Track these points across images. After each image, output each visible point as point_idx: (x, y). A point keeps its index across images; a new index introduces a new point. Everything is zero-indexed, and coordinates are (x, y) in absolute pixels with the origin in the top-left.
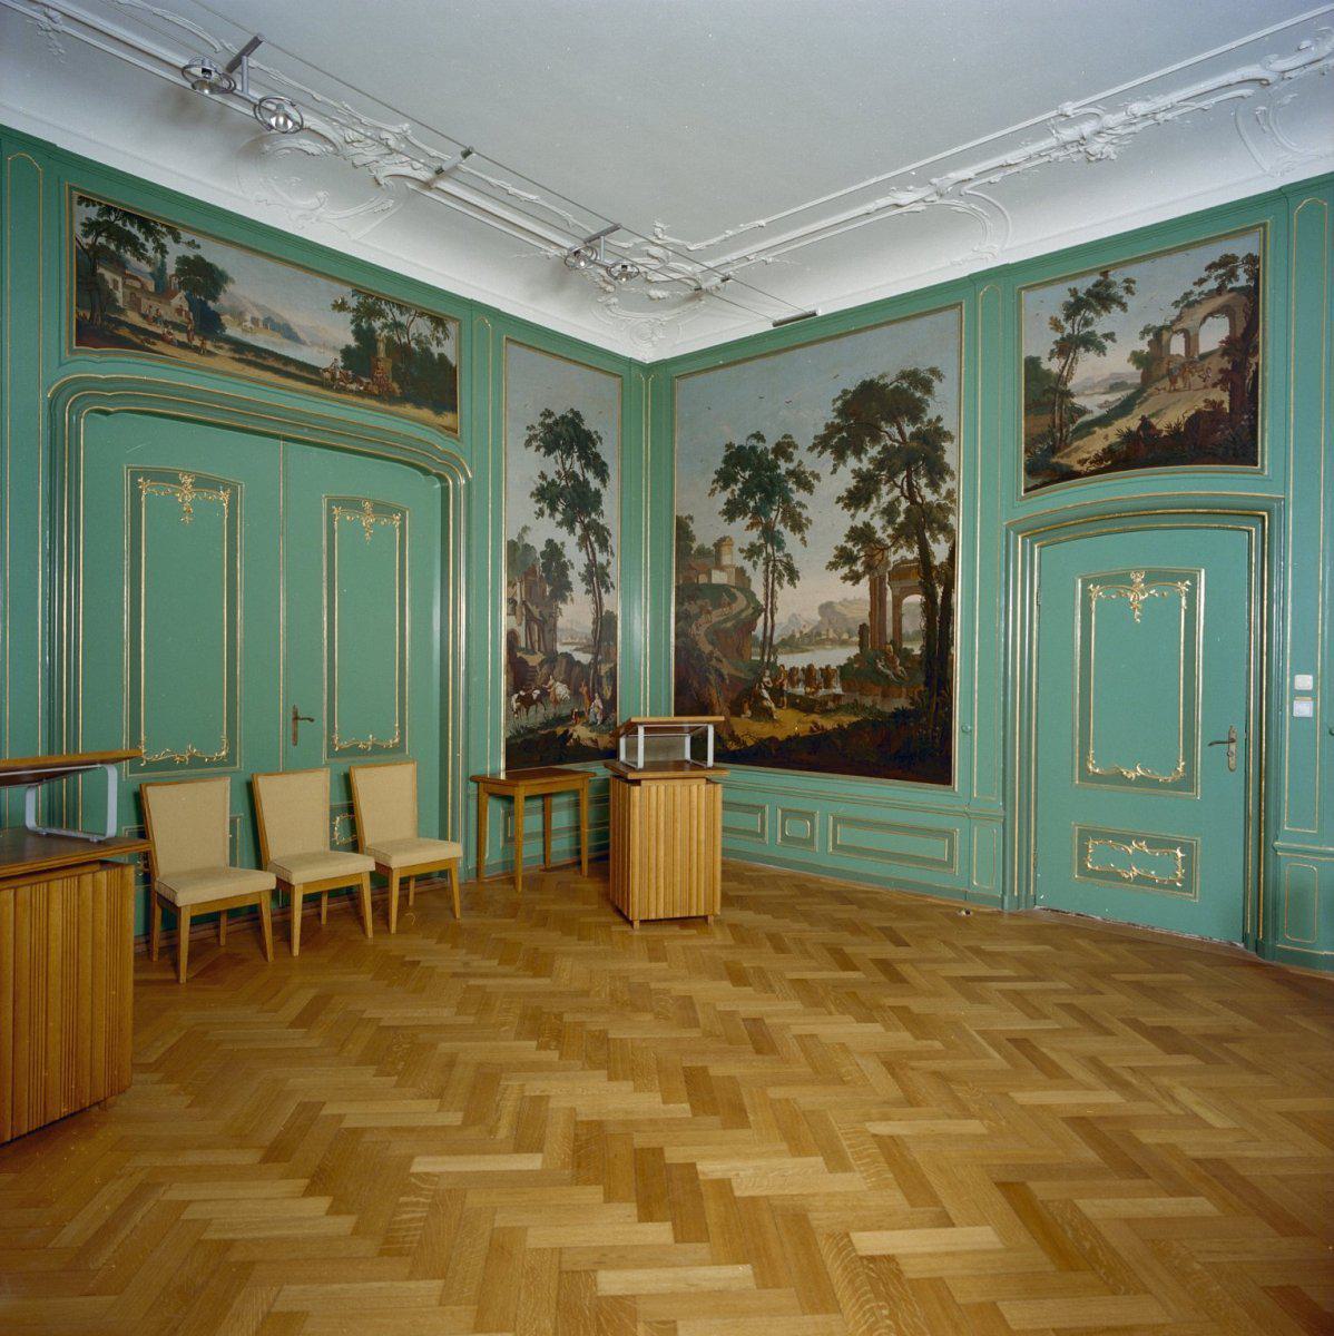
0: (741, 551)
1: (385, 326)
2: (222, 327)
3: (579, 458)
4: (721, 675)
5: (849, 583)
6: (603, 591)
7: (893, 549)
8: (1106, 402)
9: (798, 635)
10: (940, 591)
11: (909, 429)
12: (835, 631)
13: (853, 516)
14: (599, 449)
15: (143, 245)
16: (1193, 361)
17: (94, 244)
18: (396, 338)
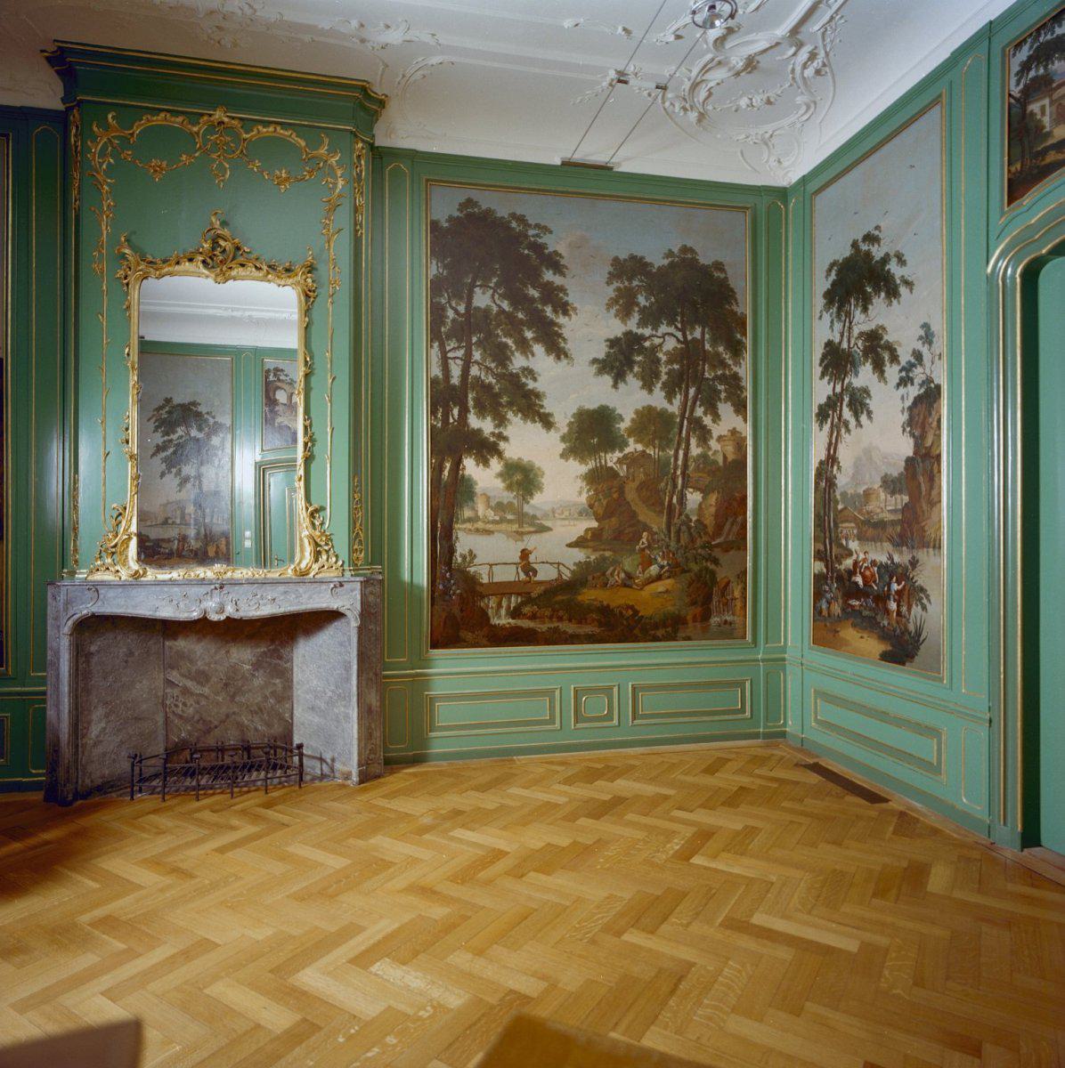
17: (1025, 86)
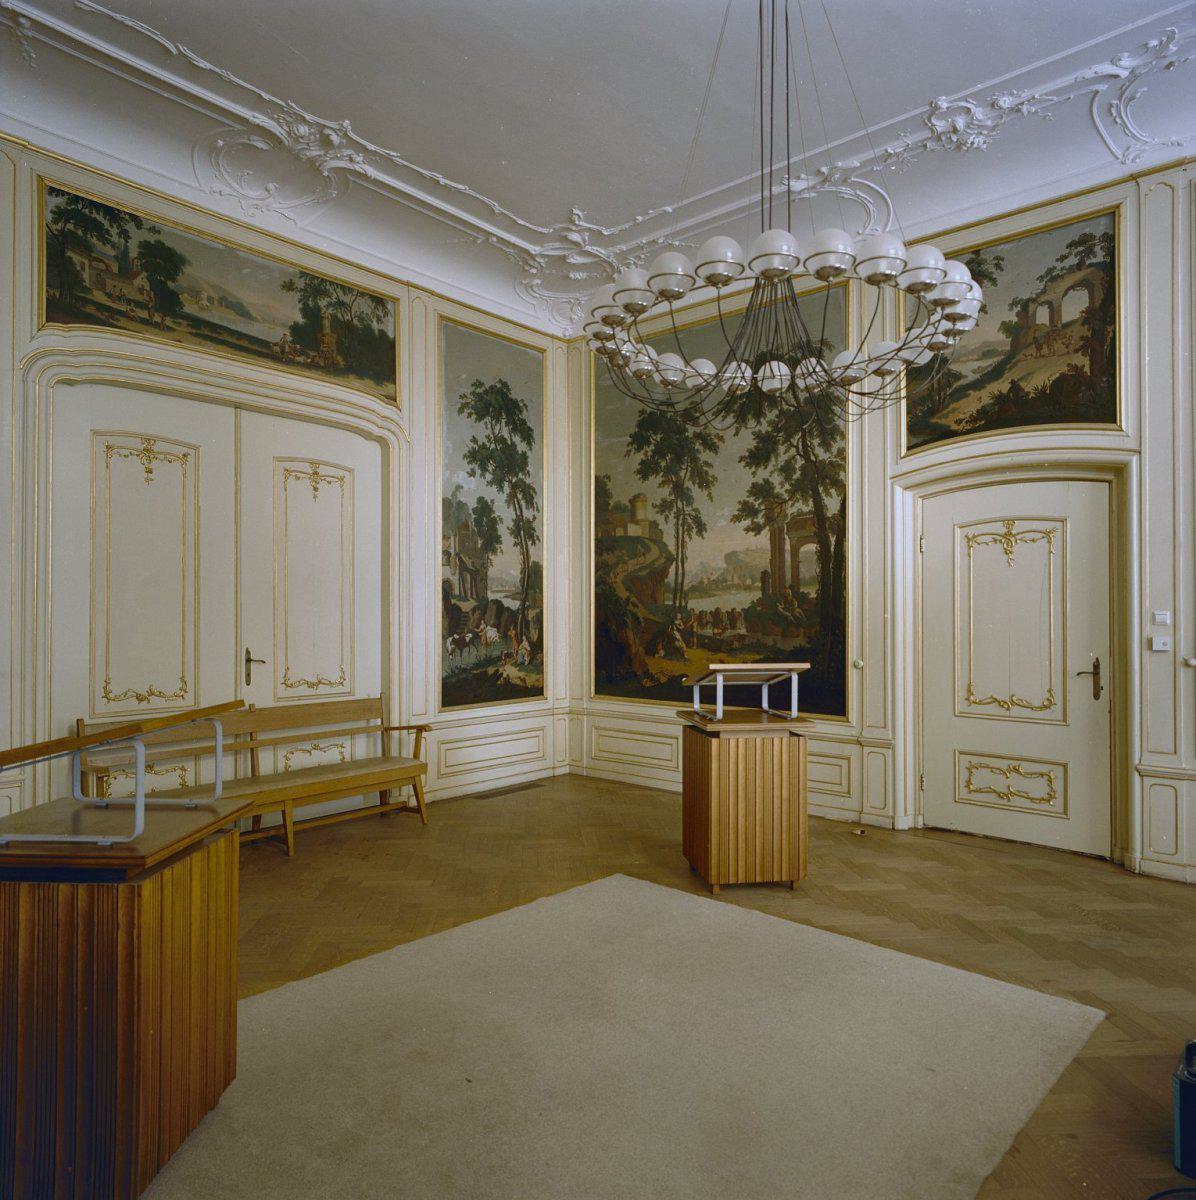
0: (654, 506)
1: (330, 304)
2: (181, 305)
3: (507, 424)
4: (637, 619)
5: (751, 534)
6: (530, 543)
7: (790, 503)
8: (979, 368)
9: (706, 581)
10: (833, 540)
12: (739, 578)
13: (754, 473)
14: (525, 415)
15: (108, 231)
16: (1057, 330)
18: (339, 315)
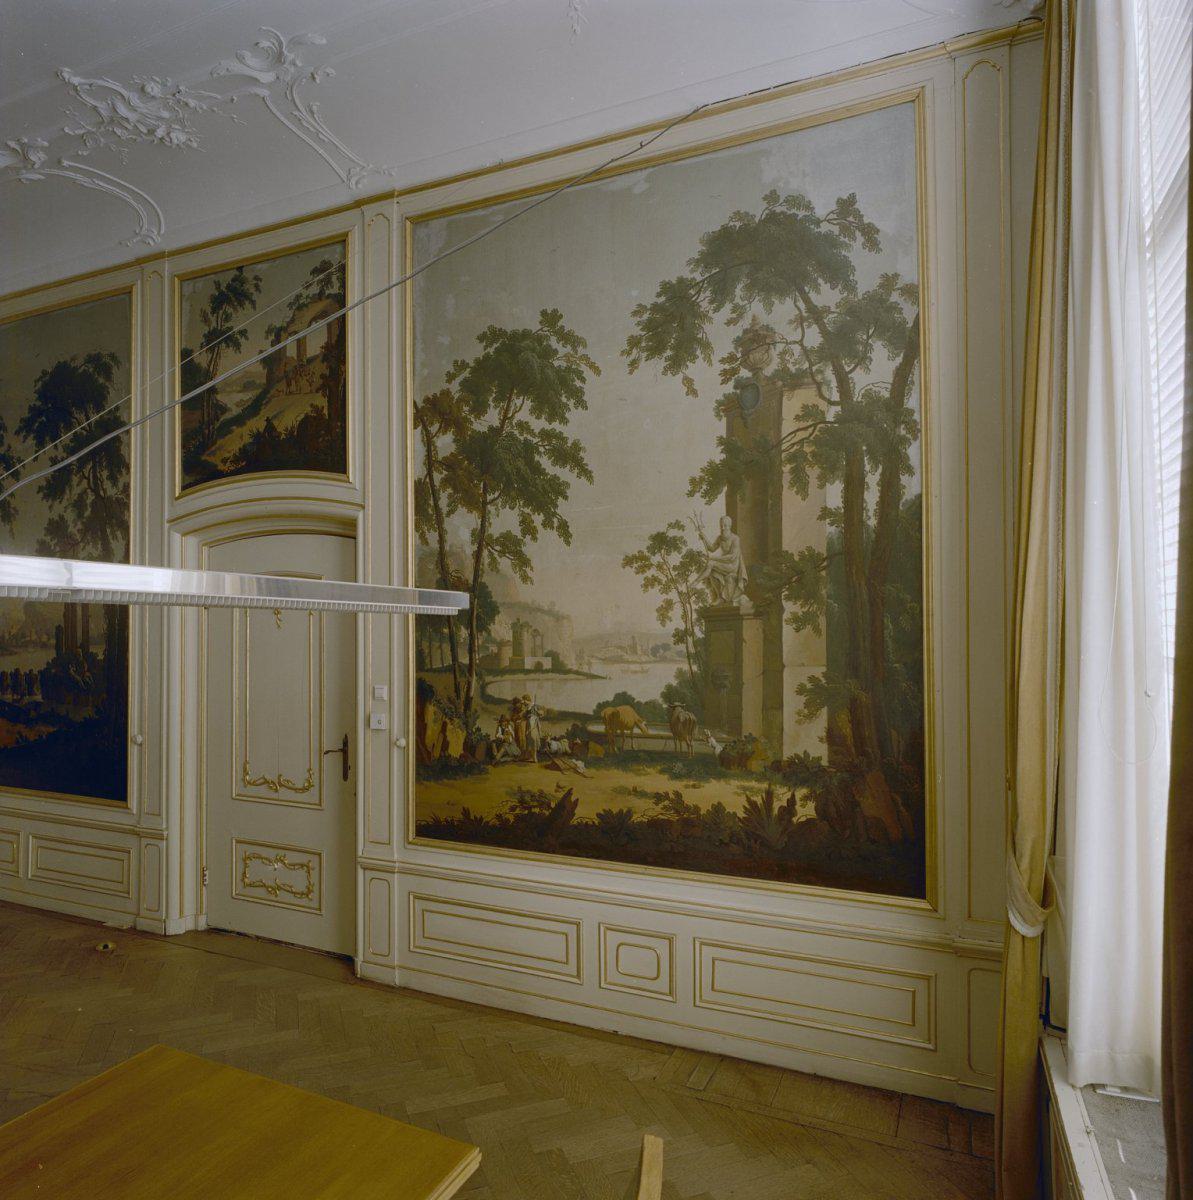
11: (94, 418)
13: (50, 507)
